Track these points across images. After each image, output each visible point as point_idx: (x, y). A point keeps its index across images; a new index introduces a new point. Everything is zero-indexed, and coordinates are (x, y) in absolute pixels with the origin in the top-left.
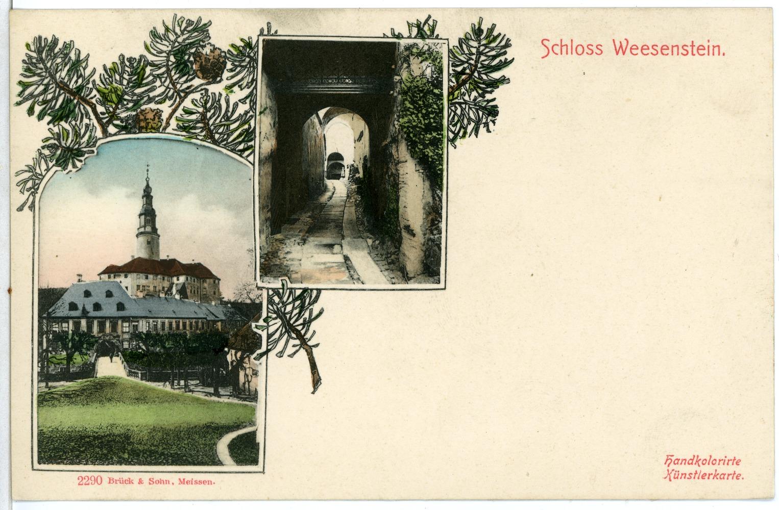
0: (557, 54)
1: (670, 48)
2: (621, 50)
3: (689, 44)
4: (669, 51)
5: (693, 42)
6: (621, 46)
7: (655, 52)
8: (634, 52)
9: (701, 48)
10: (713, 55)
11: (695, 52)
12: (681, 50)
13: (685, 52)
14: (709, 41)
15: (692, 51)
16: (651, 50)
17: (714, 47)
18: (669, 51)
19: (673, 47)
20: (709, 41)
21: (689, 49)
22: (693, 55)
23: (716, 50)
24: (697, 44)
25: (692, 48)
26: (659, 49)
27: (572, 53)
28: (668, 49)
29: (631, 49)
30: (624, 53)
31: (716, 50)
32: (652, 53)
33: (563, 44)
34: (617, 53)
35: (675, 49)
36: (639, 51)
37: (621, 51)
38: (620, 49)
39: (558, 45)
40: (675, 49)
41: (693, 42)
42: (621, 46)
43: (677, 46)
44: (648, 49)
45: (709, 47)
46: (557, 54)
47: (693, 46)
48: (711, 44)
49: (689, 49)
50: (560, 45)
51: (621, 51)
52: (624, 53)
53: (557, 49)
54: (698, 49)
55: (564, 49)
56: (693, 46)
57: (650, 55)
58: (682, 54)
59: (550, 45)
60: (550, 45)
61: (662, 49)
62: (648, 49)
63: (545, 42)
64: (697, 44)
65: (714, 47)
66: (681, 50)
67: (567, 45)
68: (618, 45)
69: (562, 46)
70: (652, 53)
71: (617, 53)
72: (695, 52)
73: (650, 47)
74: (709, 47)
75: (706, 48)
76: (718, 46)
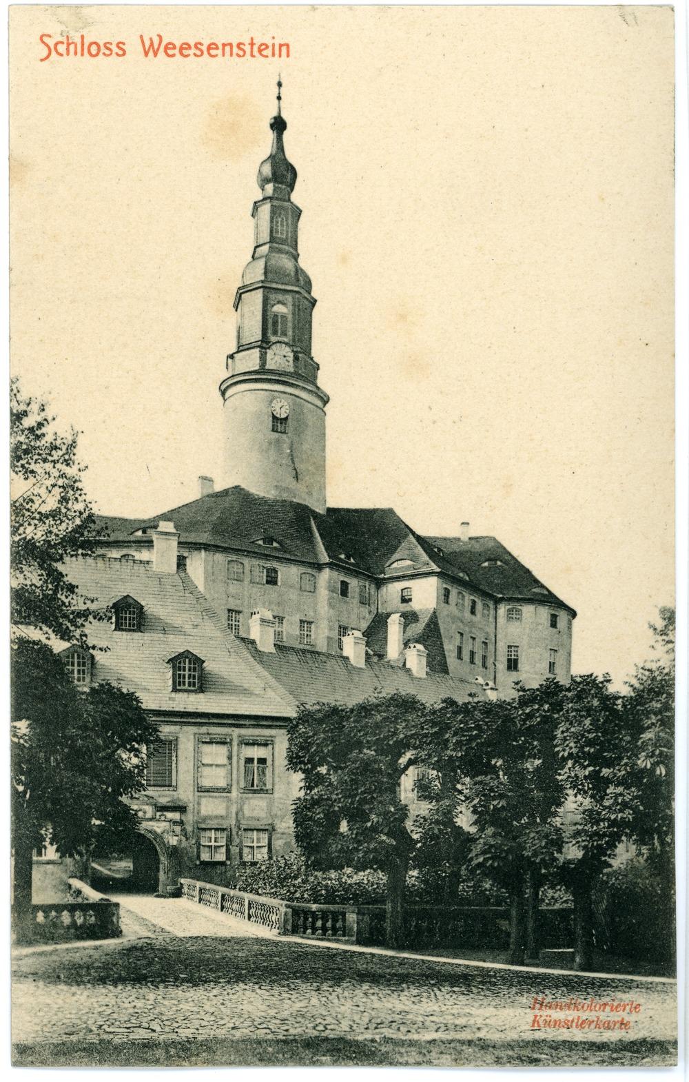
0: (61, 55)
1: (220, 47)
2: (151, 50)
3: (247, 41)
4: (219, 52)
5: (252, 39)
6: (152, 44)
7: (198, 53)
8: (170, 52)
9: (263, 47)
10: (280, 56)
12: (235, 50)
13: (241, 53)
14: (273, 38)
15: (252, 52)
16: (193, 51)
17: (281, 46)
18: (219, 52)
19: (224, 45)
20: (273, 38)
21: (247, 48)
22: (252, 56)
23: (284, 49)
24: (258, 42)
25: (252, 49)
26: (204, 48)
27: (82, 55)
28: (217, 48)
29: (166, 48)
30: (155, 54)
31: (284, 49)
32: (195, 55)
34: (146, 54)
35: (227, 49)
36: (176, 51)
37: (151, 50)
38: (150, 49)
39: (62, 43)
40: (227, 49)
41: (252, 39)
42: (152, 44)
43: (231, 45)
44: (190, 48)
45: (274, 45)
46: (61, 55)
47: (252, 44)
48: (277, 42)
49: (247, 48)
50: (64, 40)
51: (151, 53)
53: (62, 48)
54: (259, 48)
55: (72, 48)
56: (252, 44)
57: (192, 56)
58: (238, 55)
59: (51, 42)
60: (51, 42)
61: (209, 48)
62: (190, 48)
63: (45, 39)
64: (258, 42)
65: (281, 46)
66: (235, 50)
68: (147, 44)
69: (68, 44)
70: (195, 55)
71: (146, 54)
74: (274, 45)
75: (271, 48)
76: (288, 45)
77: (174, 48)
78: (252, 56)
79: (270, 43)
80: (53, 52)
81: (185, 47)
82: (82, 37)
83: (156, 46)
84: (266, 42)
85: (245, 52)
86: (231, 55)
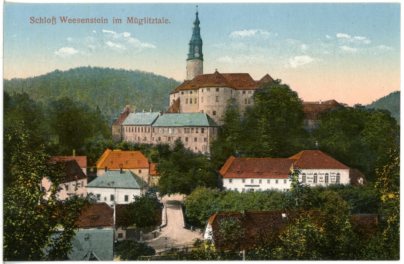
1: (85, 20)
3: (94, 19)
7: (78, 22)
8: (70, 22)
11: (96, 22)
16: (77, 21)
17: (105, 20)
19: (86, 19)
20: (102, 18)
21: (94, 21)
22: (95, 23)
23: (106, 21)
25: (95, 21)
29: (69, 21)
30: (65, 21)
31: (106, 20)
33: (41, 19)
35: (88, 20)
37: (64, 21)
40: (88, 20)
43: (88, 19)
47: (95, 19)
49: (94, 21)
51: (64, 21)
52: (65, 21)
54: (97, 20)
55: (42, 20)
58: (91, 23)
65: (105, 20)
67: (43, 19)
68: (62, 18)
72: (96, 22)
73: (76, 20)
74: (102, 20)
75: (101, 20)
76: (107, 20)
77: (71, 20)
78: (95, 23)
79: (101, 19)
80: (35, 22)
81: (74, 20)
82: (45, 18)
83: (65, 20)
84: (99, 18)
85: (93, 22)
86: (89, 22)
